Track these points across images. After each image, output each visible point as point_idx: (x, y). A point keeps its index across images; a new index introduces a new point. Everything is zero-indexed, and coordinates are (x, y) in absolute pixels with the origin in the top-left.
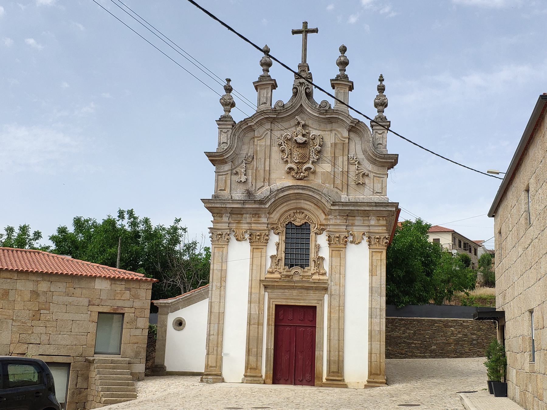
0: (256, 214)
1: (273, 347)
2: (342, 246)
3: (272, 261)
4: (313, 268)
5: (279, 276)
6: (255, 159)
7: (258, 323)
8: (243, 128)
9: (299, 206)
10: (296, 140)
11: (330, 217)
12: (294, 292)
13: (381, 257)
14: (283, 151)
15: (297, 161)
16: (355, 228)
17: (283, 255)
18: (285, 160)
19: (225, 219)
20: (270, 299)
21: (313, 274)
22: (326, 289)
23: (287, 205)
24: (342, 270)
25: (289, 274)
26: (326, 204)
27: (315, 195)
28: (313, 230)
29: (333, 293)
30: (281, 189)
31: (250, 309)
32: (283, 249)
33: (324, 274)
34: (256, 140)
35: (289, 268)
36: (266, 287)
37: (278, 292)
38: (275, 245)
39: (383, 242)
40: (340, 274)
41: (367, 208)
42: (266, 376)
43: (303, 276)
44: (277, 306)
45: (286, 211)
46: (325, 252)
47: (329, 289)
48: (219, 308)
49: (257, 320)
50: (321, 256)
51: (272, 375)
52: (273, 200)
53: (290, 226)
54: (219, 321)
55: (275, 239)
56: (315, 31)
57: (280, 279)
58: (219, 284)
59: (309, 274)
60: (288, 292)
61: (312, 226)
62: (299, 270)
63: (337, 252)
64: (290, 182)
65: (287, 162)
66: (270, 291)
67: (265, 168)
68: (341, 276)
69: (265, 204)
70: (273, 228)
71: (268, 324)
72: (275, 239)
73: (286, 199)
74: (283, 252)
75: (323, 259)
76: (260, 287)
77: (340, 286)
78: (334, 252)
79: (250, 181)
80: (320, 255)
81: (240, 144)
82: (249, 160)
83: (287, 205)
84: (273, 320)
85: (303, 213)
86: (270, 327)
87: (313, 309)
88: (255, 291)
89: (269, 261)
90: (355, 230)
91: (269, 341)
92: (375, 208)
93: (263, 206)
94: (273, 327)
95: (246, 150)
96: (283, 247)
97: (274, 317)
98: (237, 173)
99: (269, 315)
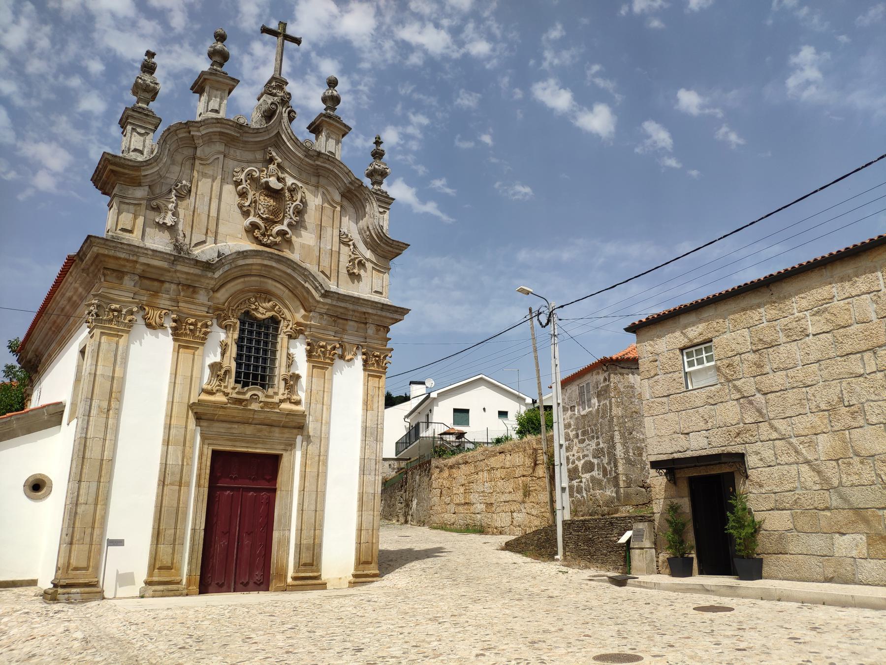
0: (190, 288)
5: (224, 399)
6: (193, 194)
7: (181, 482)
8: (180, 136)
10: (267, 183)
14: (243, 195)
15: (264, 216)
17: (234, 365)
18: (245, 209)
20: (204, 438)
23: (244, 282)
24: (325, 399)
27: (295, 275)
30: (243, 252)
31: (166, 455)
32: (234, 355)
34: (197, 162)
35: (243, 387)
36: (199, 418)
38: (219, 346)
44: (214, 452)
45: (242, 291)
48: (103, 451)
49: (178, 476)
51: (198, 578)
52: (226, 268)
53: (247, 319)
54: (100, 477)
58: (105, 405)
60: (237, 429)
61: (283, 324)
64: (248, 245)
70: (218, 317)
71: (198, 485)
74: (233, 360)
76: (187, 417)
80: (293, 370)
82: (184, 194)
84: (208, 477)
85: (269, 301)
86: (202, 489)
89: (207, 372)
92: (379, 313)
93: (210, 274)
94: (206, 490)
96: (233, 350)
97: (208, 471)
99: (200, 469)
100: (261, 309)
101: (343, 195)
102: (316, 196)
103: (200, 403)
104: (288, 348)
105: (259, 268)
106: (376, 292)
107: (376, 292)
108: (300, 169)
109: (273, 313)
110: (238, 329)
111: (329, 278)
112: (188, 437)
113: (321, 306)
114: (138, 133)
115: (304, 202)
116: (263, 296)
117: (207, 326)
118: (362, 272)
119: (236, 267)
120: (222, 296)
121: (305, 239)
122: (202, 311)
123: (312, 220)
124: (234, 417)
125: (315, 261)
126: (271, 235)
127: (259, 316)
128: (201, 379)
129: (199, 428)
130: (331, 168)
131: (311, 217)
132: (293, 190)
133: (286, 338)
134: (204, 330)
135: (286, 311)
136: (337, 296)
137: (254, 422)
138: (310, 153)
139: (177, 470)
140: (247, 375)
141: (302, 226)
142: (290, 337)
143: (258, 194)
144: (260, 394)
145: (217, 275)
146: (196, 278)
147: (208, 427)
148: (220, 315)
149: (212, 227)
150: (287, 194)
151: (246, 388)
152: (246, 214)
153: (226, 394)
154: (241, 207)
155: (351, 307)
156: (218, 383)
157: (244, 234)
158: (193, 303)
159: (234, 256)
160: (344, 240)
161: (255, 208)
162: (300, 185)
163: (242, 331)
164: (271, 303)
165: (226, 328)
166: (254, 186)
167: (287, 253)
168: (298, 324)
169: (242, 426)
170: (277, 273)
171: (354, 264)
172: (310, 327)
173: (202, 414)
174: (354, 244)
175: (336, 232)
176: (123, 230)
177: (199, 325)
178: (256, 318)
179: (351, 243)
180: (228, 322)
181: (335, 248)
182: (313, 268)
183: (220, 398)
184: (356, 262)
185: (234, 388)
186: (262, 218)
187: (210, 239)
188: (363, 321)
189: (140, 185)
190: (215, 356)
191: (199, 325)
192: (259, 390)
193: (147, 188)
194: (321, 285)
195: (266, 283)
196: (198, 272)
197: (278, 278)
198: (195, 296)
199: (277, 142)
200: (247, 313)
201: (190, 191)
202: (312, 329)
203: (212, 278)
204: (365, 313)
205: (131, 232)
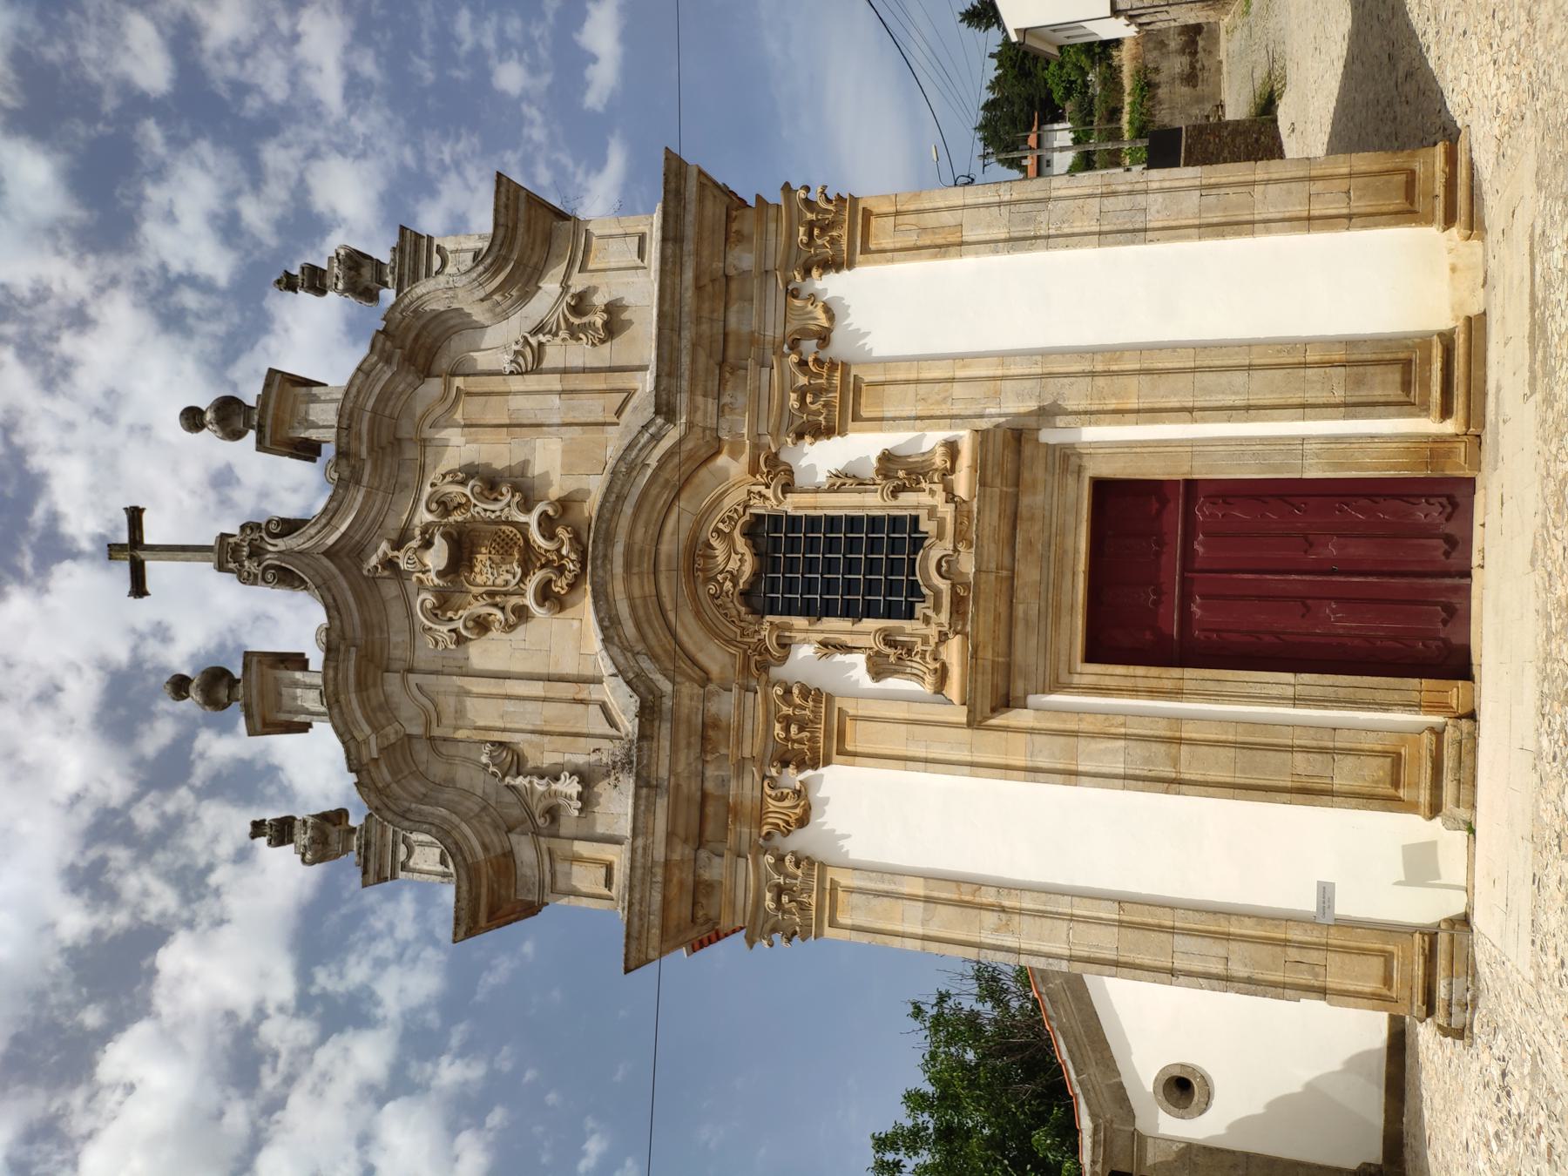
1: (1288, 677)
2: (837, 380)
4: (924, 498)
5: (955, 643)
6: (505, 737)
10: (440, 574)
13: (886, 215)
14: (482, 625)
15: (519, 571)
16: (770, 333)
17: (870, 624)
18: (512, 619)
19: (715, 870)
28: (771, 503)
30: (603, 629)
33: (952, 449)
36: (1006, 701)
37: (1027, 650)
39: (827, 211)
40: (952, 380)
41: (689, 275)
42: (1433, 707)
43: (959, 536)
45: (698, 614)
46: (858, 447)
47: (1017, 424)
49: (1155, 747)
52: (646, 664)
53: (761, 598)
56: (135, 516)
59: (947, 512)
60: (1028, 605)
61: (759, 507)
63: (863, 400)
65: (522, 614)
67: (535, 699)
68: (960, 374)
70: (764, 667)
73: (654, 611)
75: (887, 458)
76: (1006, 729)
77: (1003, 378)
78: (865, 413)
79: (580, 759)
81: (449, 795)
87: (1103, 489)
88: (1018, 751)
89: (893, 683)
90: (779, 332)
91: (1256, 690)
93: (667, 703)
95: (473, 775)
98: (553, 813)
100: (733, 565)
101: (427, 372)
102: (445, 445)
104: (817, 490)
105: (635, 579)
106: (641, 253)
107: (641, 253)
108: (396, 488)
109: (737, 533)
110: (785, 619)
111: (630, 393)
112: (1055, 725)
113: (699, 416)
114: (409, 856)
115: (469, 472)
118: (599, 300)
120: (715, 658)
121: (549, 461)
122: (755, 705)
123: (503, 448)
124: (997, 618)
125: (593, 434)
126: (558, 551)
127: (748, 569)
128: (910, 699)
129: (1032, 699)
130: (367, 416)
131: (497, 453)
132: (444, 506)
133: (792, 499)
135: (728, 503)
136: (664, 382)
137: (1007, 562)
138: (346, 474)
139: (1139, 749)
140: (892, 588)
141: (523, 475)
142: (788, 488)
143: (475, 590)
144: (935, 555)
145: (667, 687)
146: (683, 729)
148: (758, 663)
149: (567, 690)
150: (457, 517)
151: (925, 590)
152: (522, 614)
153: (943, 638)
154: (509, 627)
155: (687, 335)
157: (569, 613)
158: (741, 727)
159: (615, 651)
160: (531, 361)
161: (506, 594)
162: (428, 490)
163: (790, 610)
164: (712, 541)
165: (785, 645)
166: (457, 599)
167: (591, 507)
168: (754, 469)
169: (1020, 594)
171: (584, 328)
173: (995, 696)
174: (536, 331)
175: (516, 383)
176: (608, 882)
177: (787, 710)
178: (756, 575)
179: (533, 341)
180: (771, 644)
181: (554, 382)
182: (613, 443)
183: (953, 652)
184: (576, 321)
185: (927, 620)
186: (525, 574)
187: (594, 692)
188: (721, 288)
189: (509, 855)
190: (854, 666)
191: (787, 710)
192: (925, 558)
193: (514, 837)
194: (645, 427)
195: (669, 556)
196: (665, 728)
197: (653, 530)
198: (724, 724)
199: (348, 553)
200: (746, 596)
201: (501, 744)
202: (763, 430)
204: (699, 288)
205: (609, 868)
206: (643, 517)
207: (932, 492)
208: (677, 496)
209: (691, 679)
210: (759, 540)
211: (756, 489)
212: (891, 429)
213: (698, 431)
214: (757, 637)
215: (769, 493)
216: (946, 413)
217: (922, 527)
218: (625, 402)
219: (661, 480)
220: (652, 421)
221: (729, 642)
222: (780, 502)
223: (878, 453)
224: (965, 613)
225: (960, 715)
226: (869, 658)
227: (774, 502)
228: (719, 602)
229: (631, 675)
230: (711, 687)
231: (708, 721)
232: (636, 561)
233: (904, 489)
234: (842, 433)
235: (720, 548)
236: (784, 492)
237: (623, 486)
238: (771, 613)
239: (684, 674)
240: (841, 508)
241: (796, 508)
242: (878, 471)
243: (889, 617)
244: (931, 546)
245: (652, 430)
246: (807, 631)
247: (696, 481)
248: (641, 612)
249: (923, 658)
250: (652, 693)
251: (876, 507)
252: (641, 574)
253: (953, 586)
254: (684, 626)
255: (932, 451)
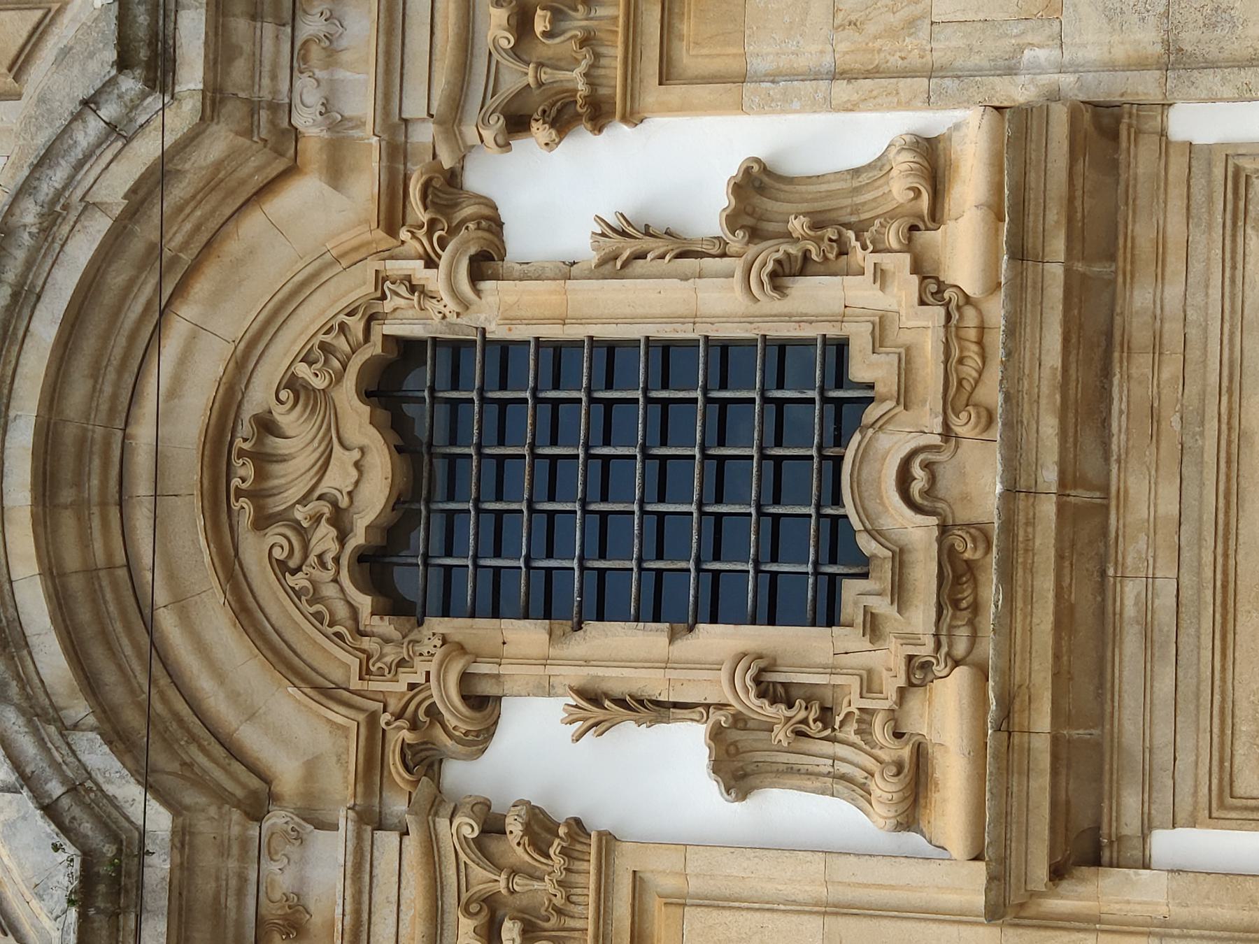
3: (788, 774)
9: (187, 469)
11: (306, 120)
12: (1139, 511)
21: (932, 288)
22: (1106, 129)
25: (924, 574)
26: (146, 150)
28: (439, 307)
29: (1147, 39)
32: (647, 639)
33: (932, 160)
43: (956, 396)
47: (1106, 88)
50: (720, 200)
52: (97, 756)
55: (536, 749)
57: (982, 672)
59: (923, 329)
61: (407, 322)
62: (882, 448)
66: (1131, 802)
69: (132, 847)
70: (424, 762)
72: (536, 749)
75: (756, 186)
78: (688, 58)
80: (707, 209)
83: (180, 603)
85: (266, 425)
89: (786, 808)
93: (159, 866)
96: (625, 649)
100: (338, 479)
103: (992, 847)
105: (68, 522)
109: (347, 396)
113: (239, 70)
116: (245, 471)
117: (492, 826)
119: (89, 682)
129: (1168, 843)
134: (514, 846)
142: (485, 264)
147: (1148, 785)
148: (413, 755)
151: (867, 545)
153: (918, 673)
156: (849, 733)
165: (483, 704)
168: (392, 217)
170: (77, 393)
172: (395, 134)
177: (483, 878)
178: (404, 506)
183: (946, 716)
185: (873, 626)
191: (483, 878)
192: (862, 457)
194: (90, 103)
198: (316, 920)
200: (375, 567)
203: (183, 838)
206: (89, 345)
207: (880, 275)
208: (181, 290)
209: (221, 796)
210: (409, 409)
211: (395, 267)
212: (766, 106)
213: (233, 110)
214: (405, 678)
215: (434, 280)
216: (914, 59)
217: (859, 371)
218: (37, 35)
219: (137, 247)
220: (112, 82)
221: (327, 692)
222: (466, 305)
223: (733, 168)
224: (975, 608)
225: (968, 885)
226: (716, 735)
227: (452, 306)
228: (299, 581)
229: (55, 788)
230: (277, 819)
231: (273, 911)
232: (67, 473)
233: (804, 266)
234: (632, 117)
235: (298, 434)
236: (476, 276)
237: (29, 264)
238: (446, 613)
239: (201, 783)
240: (632, 320)
241: (510, 320)
242: (733, 220)
243: (772, 622)
244: (880, 425)
245: (109, 111)
246: (545, 661)
247: (233, 247)
248: (84, 614)
249: (864, 731)
250: (114, 837)
251: (727, 318)
252: (81, 507)
253: (944, 529)
254: (202, 649)
255: (879, 165)
